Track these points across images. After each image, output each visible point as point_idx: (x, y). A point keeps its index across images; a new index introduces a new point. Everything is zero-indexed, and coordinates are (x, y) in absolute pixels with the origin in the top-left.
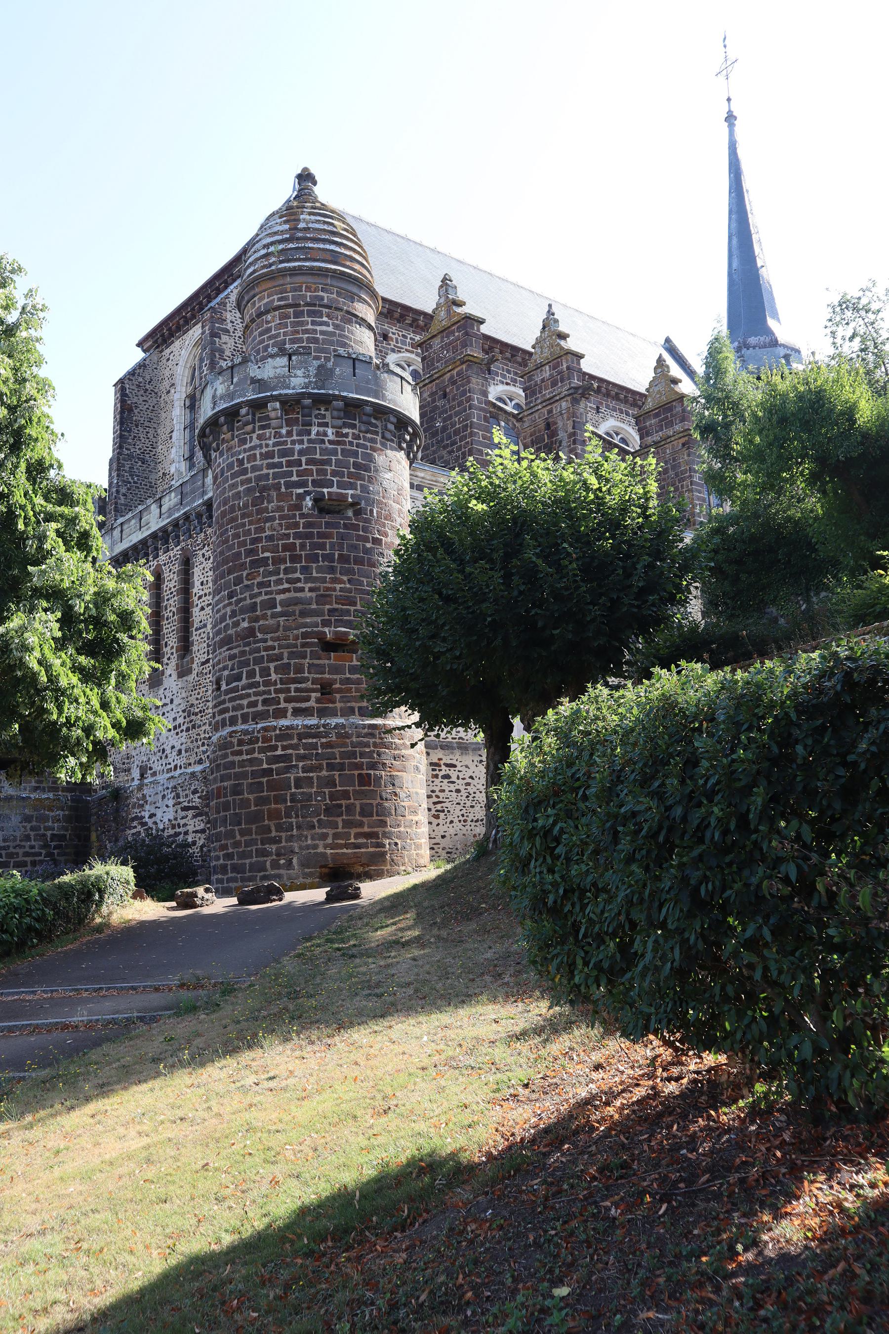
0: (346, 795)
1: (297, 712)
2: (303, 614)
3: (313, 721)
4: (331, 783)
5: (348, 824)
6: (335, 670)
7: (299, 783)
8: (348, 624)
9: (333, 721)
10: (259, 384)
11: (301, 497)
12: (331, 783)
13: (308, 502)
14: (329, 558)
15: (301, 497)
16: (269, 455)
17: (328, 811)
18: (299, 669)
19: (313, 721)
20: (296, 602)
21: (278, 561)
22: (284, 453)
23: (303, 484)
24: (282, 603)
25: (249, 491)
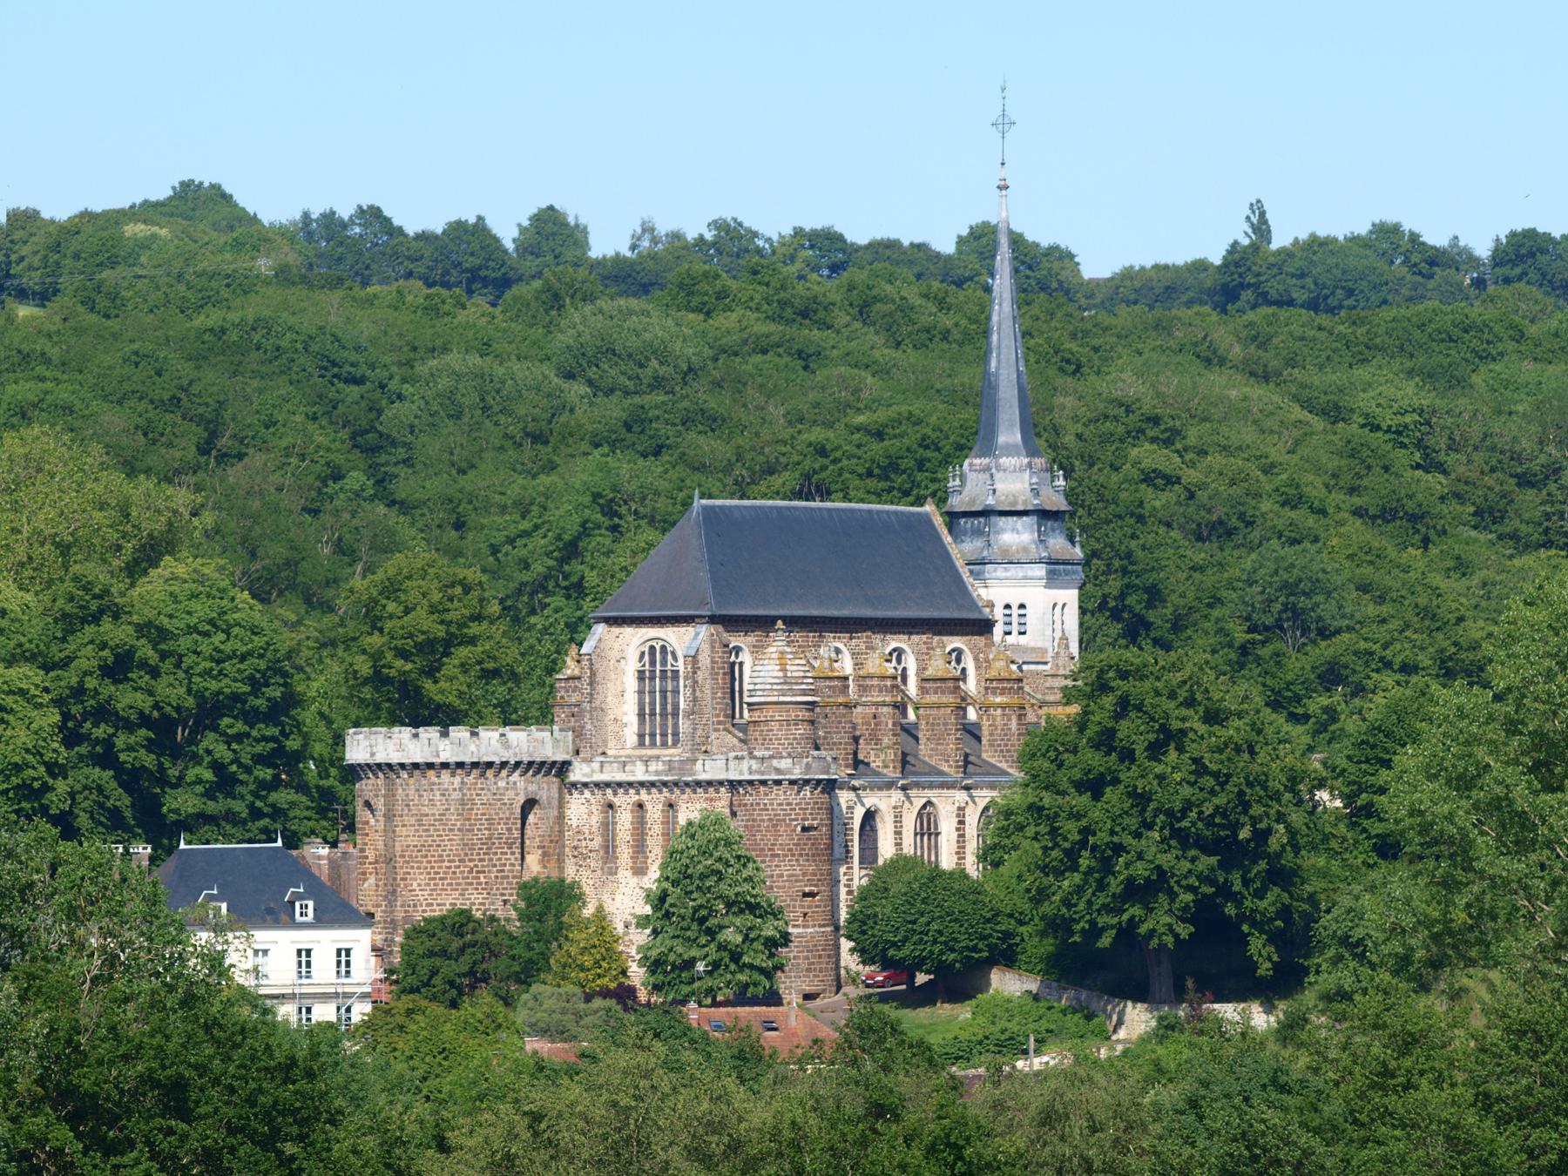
0: (813, 963)
1: (794, 926)
2: (796, 881)
3: (800, 930)
4: (807, 958)
5: (815, 976)
6: (809, 907)
7: (795, 958)
8: (816, 886)
9: (811, 930)
10: (778, 771)
11: (796, 826)
12: (807, 958)
13: (799, 829)
14: (807, 855)
15: (796, 826)
16: (781, 804)
17: (808, 970)
18: (794, 907)
19: (800, 930)
20: (793, 875)
21: (786, 856)
22: (788, 804)
23: (796, 820)
24: (788, 876)
25: (770, 820)
